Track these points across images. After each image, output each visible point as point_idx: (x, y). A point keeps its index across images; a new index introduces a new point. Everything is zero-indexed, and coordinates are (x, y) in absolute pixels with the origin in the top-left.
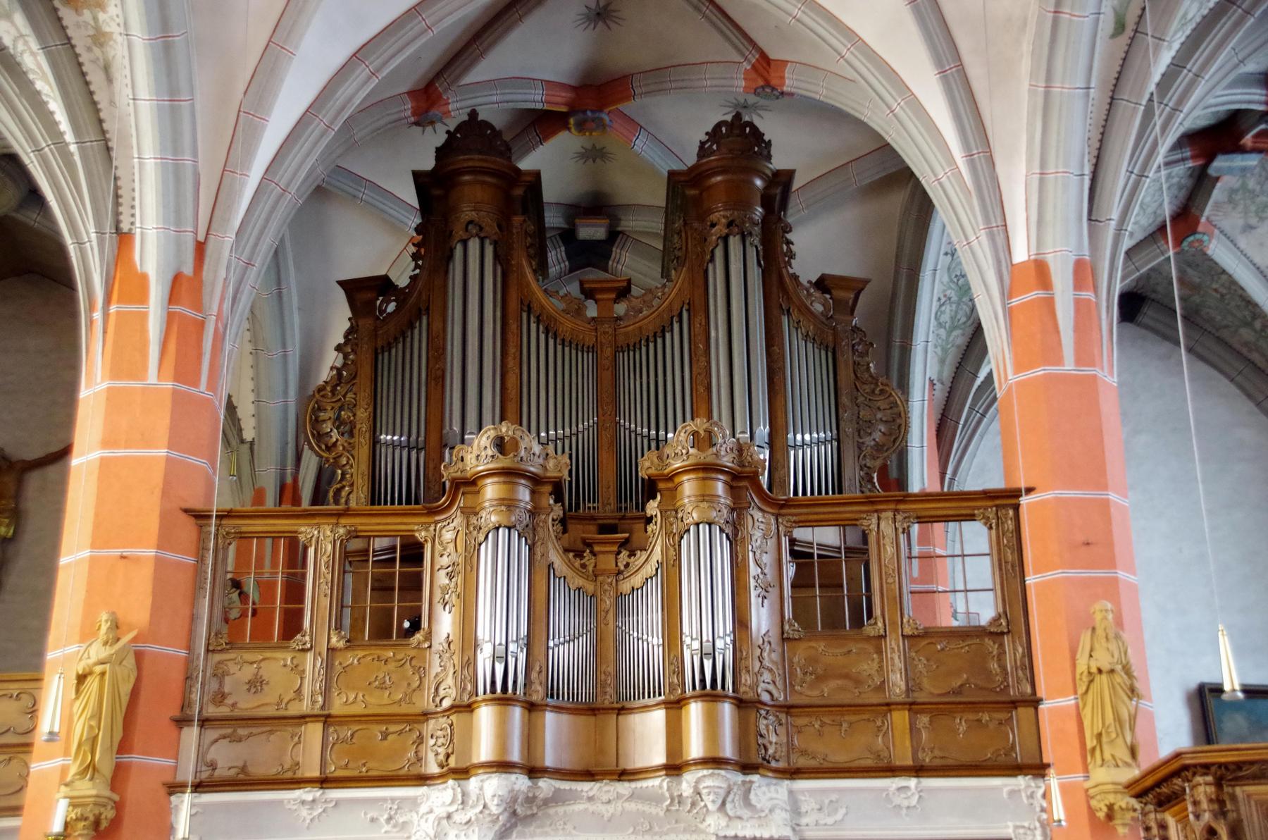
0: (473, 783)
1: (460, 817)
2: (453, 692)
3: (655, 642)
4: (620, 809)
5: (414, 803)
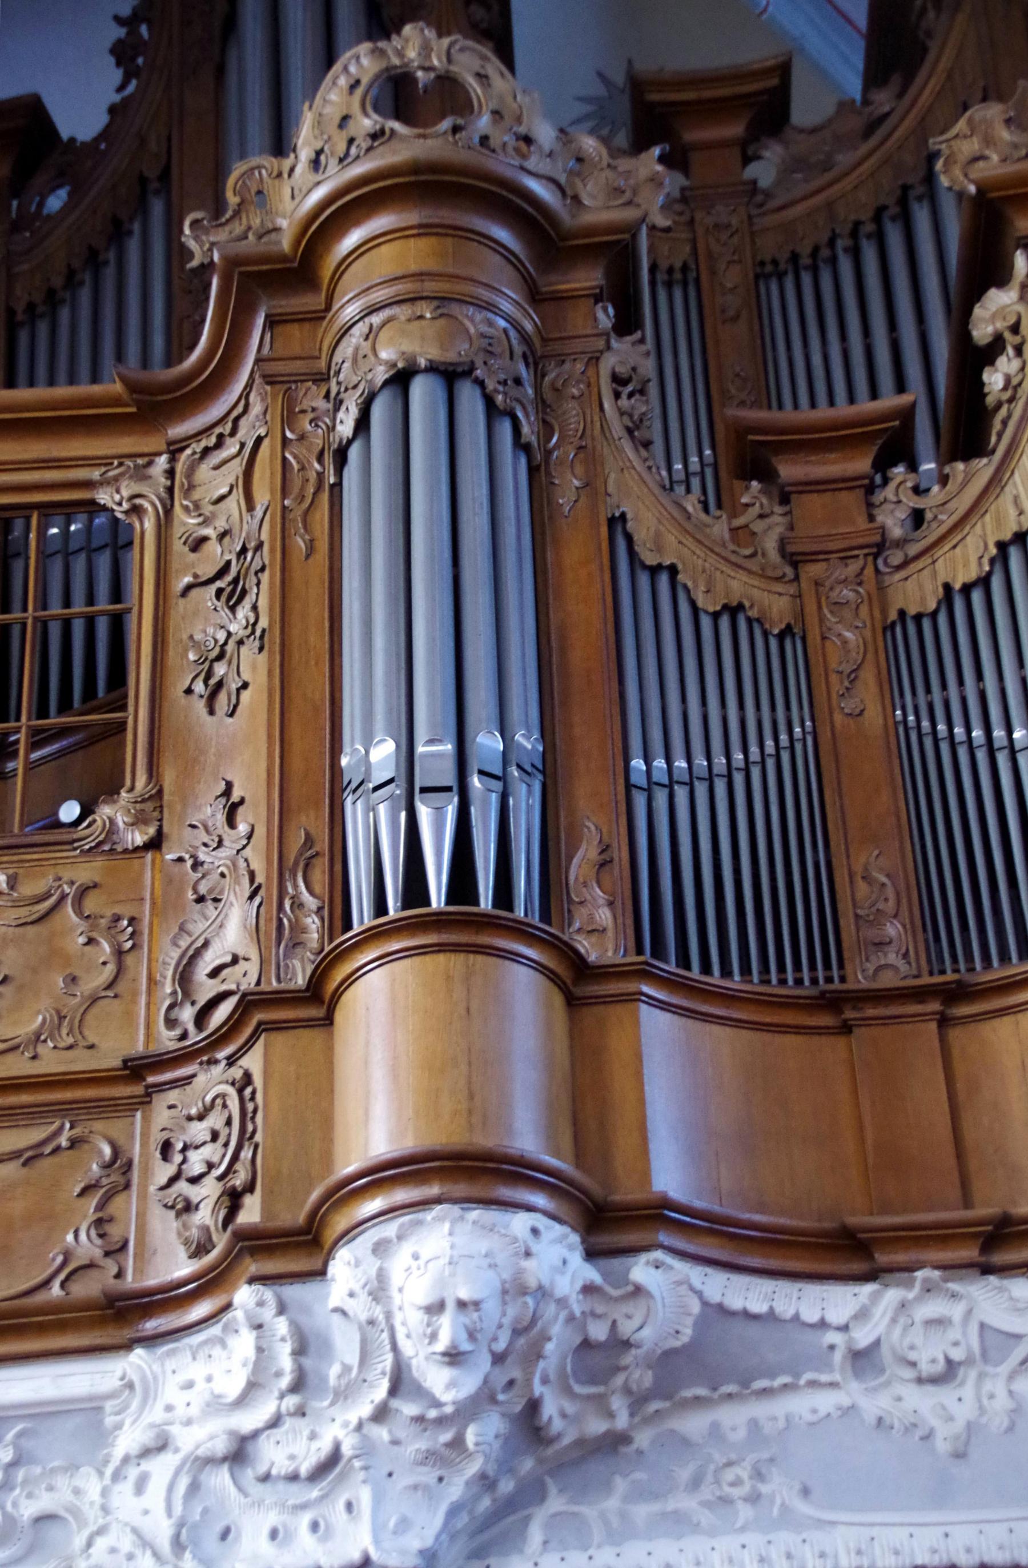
1: (289, 1450)
4: (1002, 1402)
5: (89, 1415)
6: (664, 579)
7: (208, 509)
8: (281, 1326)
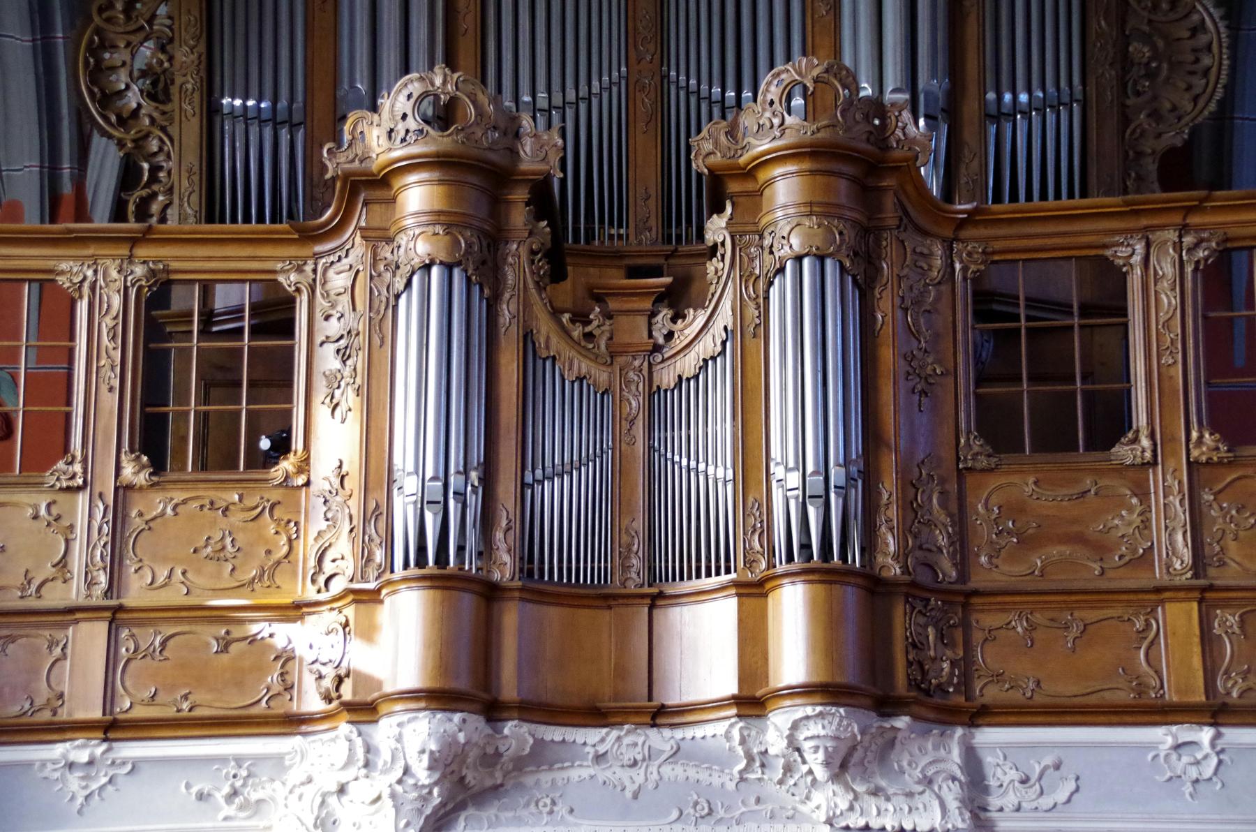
0: (384, 731)
2: (348, 567)
3: (720, 474)
4: (655, 776)
6: (548, 364)
7: (333, 297)
8: (359, 742)
